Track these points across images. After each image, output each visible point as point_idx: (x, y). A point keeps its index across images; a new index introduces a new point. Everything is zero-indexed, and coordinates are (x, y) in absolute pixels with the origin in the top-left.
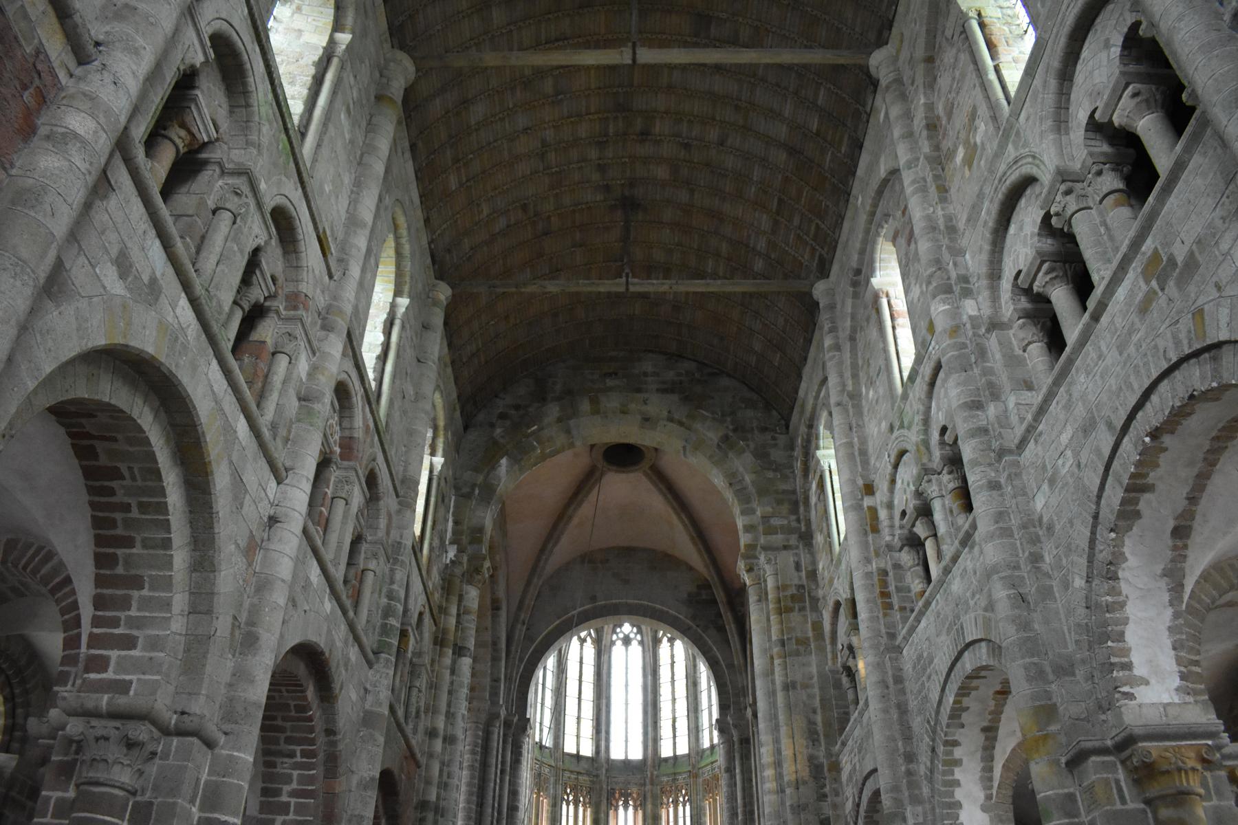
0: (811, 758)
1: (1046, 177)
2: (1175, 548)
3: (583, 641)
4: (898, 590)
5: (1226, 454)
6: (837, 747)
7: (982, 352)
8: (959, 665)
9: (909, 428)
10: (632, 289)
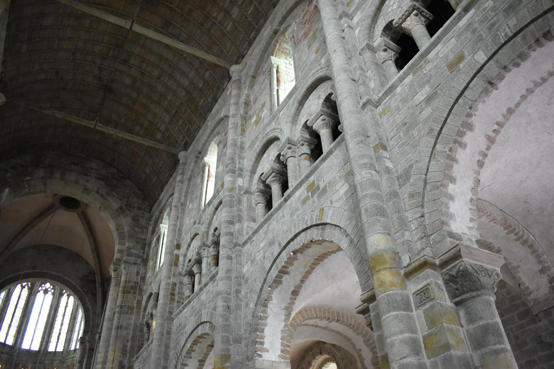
0: (120, 362)
1: (283, 139)
2: (291, 299)
3: (23, 287)
4: (179, 293)
5: (319, 266)
6: (134, 359)
7: (240, 202)
8: (196, 331)
9: (202, 225)
10: (97, 128)
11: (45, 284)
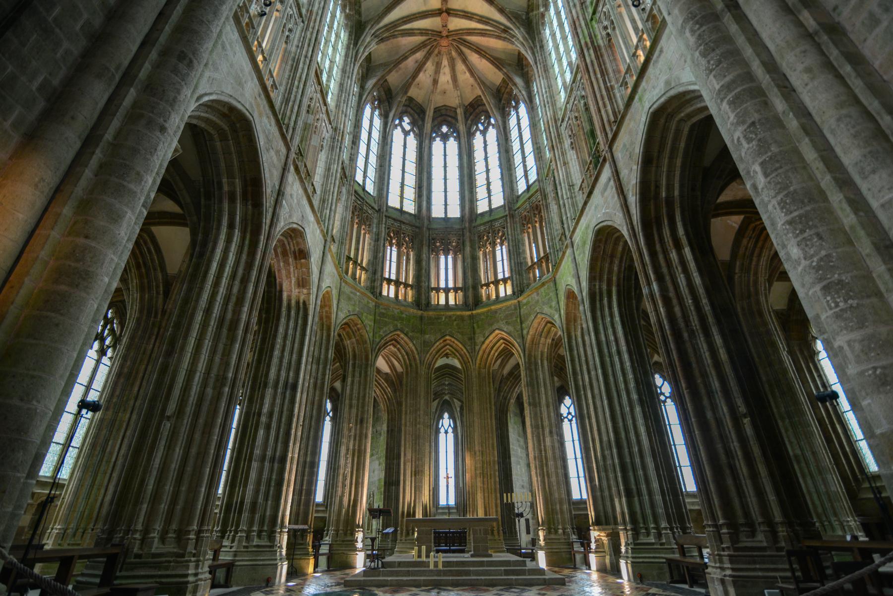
11: (440, 126)
